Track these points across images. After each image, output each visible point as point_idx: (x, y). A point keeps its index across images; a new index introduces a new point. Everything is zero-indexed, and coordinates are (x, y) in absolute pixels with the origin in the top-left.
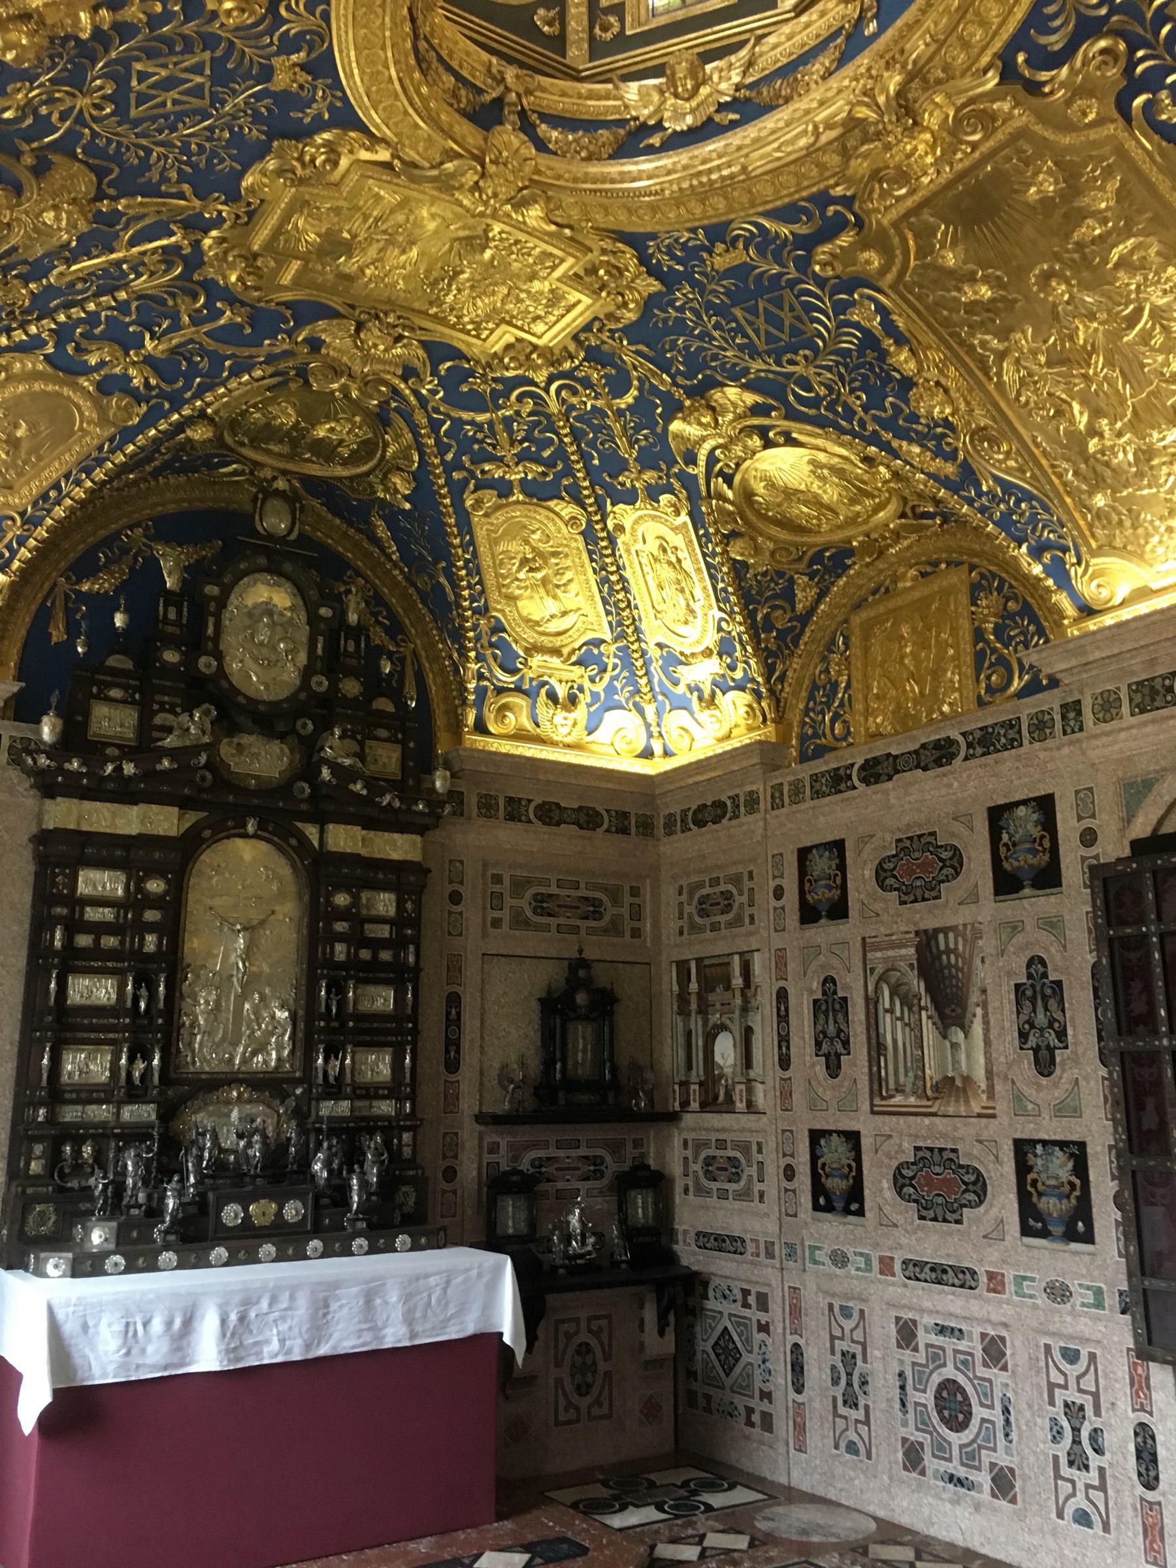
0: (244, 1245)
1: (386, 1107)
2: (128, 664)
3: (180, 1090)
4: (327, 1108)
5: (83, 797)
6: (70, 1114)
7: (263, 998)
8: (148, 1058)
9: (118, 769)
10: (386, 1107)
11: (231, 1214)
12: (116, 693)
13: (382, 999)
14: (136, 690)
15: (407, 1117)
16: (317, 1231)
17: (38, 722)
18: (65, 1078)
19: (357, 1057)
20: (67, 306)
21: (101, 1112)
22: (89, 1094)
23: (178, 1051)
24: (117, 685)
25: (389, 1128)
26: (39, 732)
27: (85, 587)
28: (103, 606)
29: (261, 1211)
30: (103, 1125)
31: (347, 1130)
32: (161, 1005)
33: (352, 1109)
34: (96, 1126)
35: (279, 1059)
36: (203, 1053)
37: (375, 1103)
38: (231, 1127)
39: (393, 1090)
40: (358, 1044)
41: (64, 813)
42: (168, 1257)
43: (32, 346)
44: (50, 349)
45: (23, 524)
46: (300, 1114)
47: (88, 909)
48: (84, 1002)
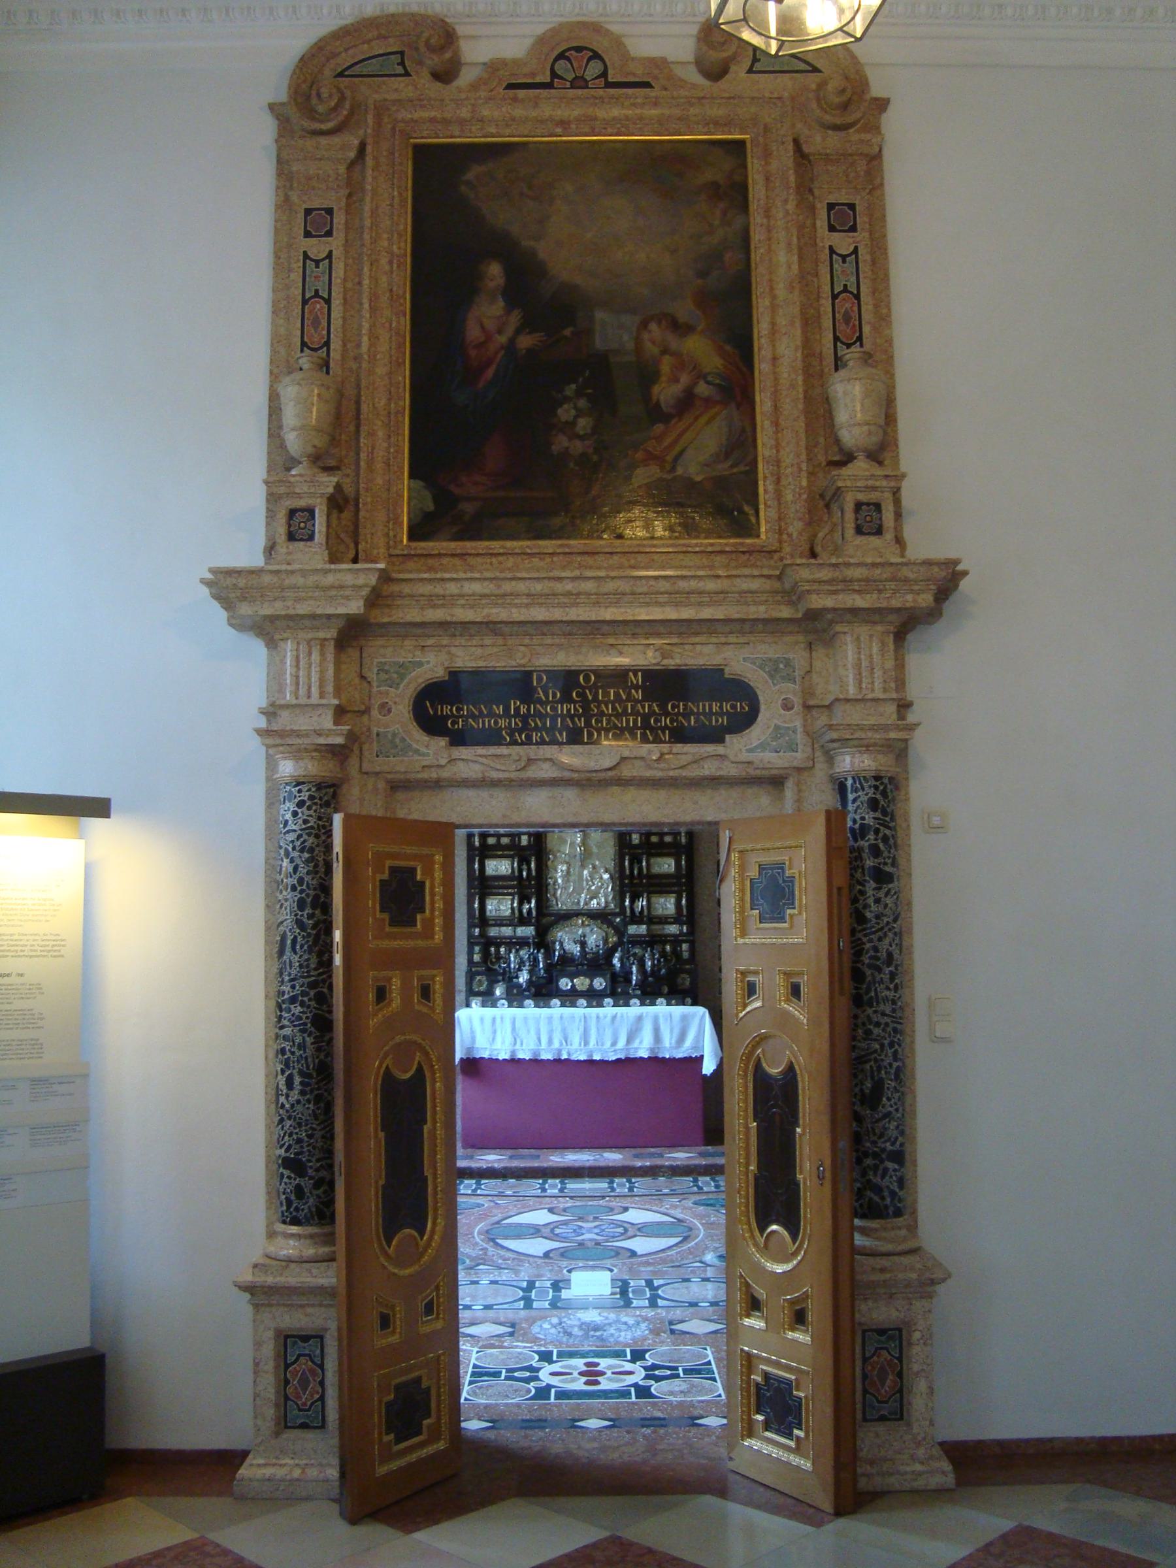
0: (570, 998)
1: (673, 929)
3: (546, 921)
4: (632, 929)
6: (493, 932)
7: (594, 867)
8: (529, 902)
10: (673, 929)
11: (565, 984)
13: (666, 865)
15: (685, 935)
16: (613, 994)
18: (488, 913)
19: (654, 899)
21: (507, 931)
22: (500, 922)
23: (548, 900)
25: (676, 941)
29: (581, 983)
30: (511, 938)
31: (644, 942)
32: (534, 873)
33: (648, 930)
34: (505, 938)
35: (606, 902)
36: (562, 900)
37: (667, 927)
38: (567, 940)
39: (677, 920)
40: (649, 893)
42: (529, 1002)
46: (620, 932)
48: (494, 873)
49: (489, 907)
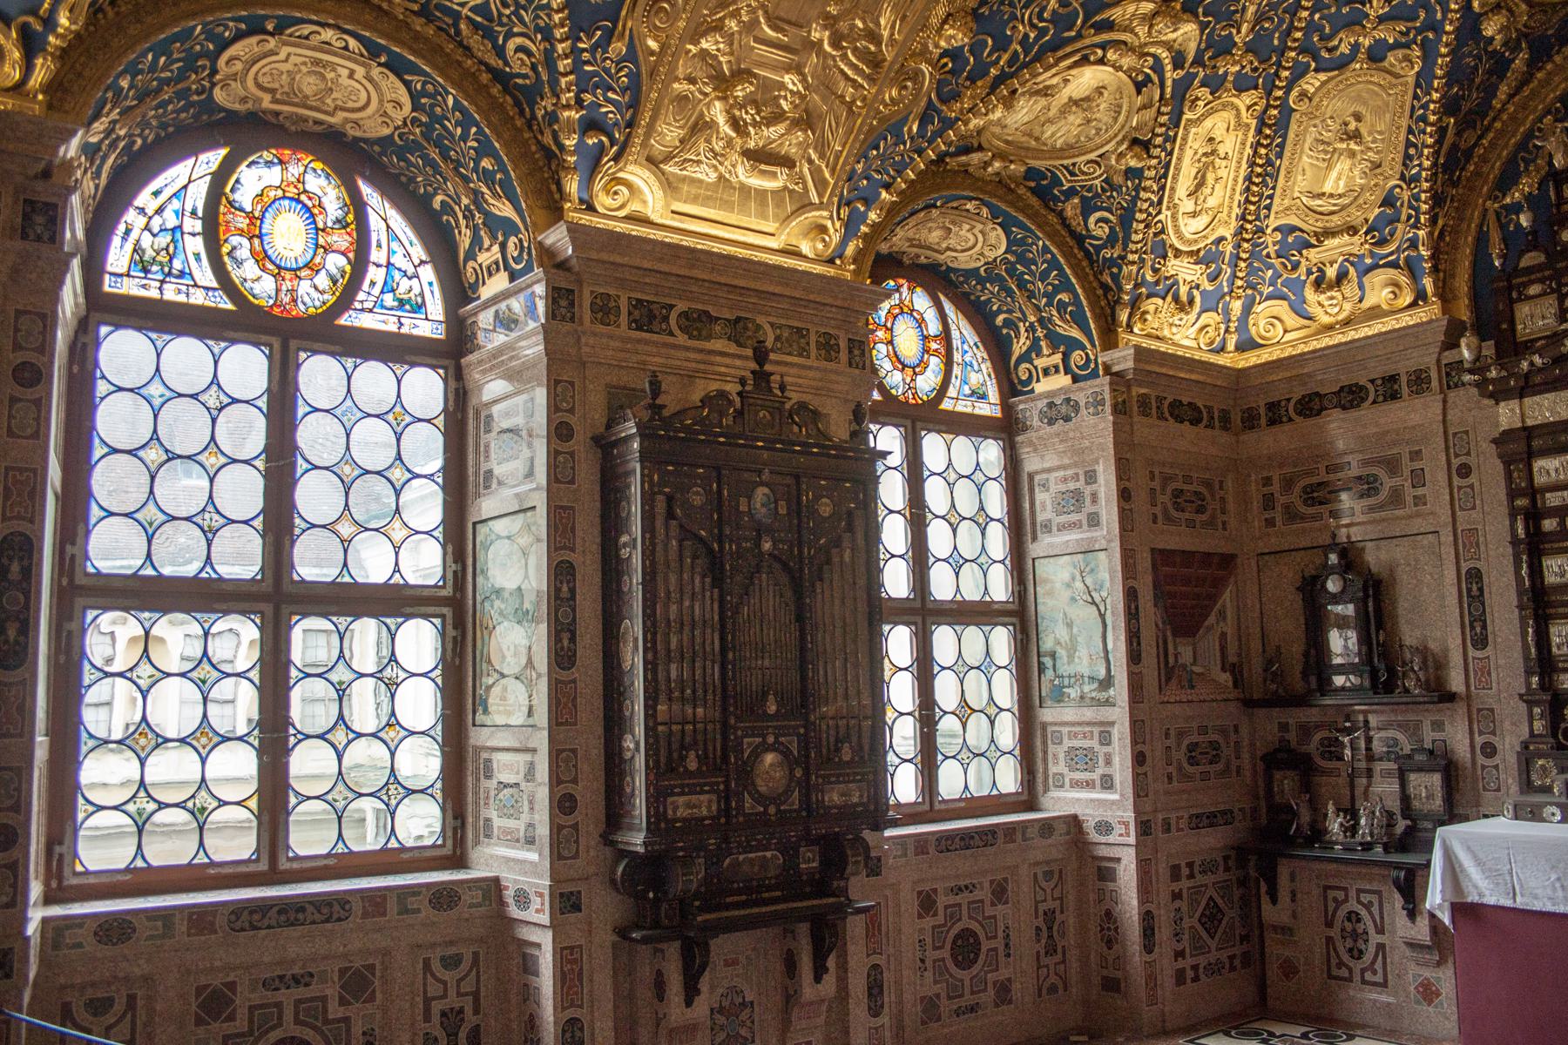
2: (1542, 258)
5: (1521, 397)
9: (1532, 364)
12: (1534, 290)
14: (1551, 278)
17: (1458, 346)
18: (1555, 650)
20: (1289, 34)
24: (1532, 282)
26: (1461, 353)
27: (1508, 200)
28: (1516, 208)
41: (1507, 415)
43: (1299, 73)
44: (1313, 65)
45: (1409, 186)
47: (1548, 495)
49: (1556, 640)
